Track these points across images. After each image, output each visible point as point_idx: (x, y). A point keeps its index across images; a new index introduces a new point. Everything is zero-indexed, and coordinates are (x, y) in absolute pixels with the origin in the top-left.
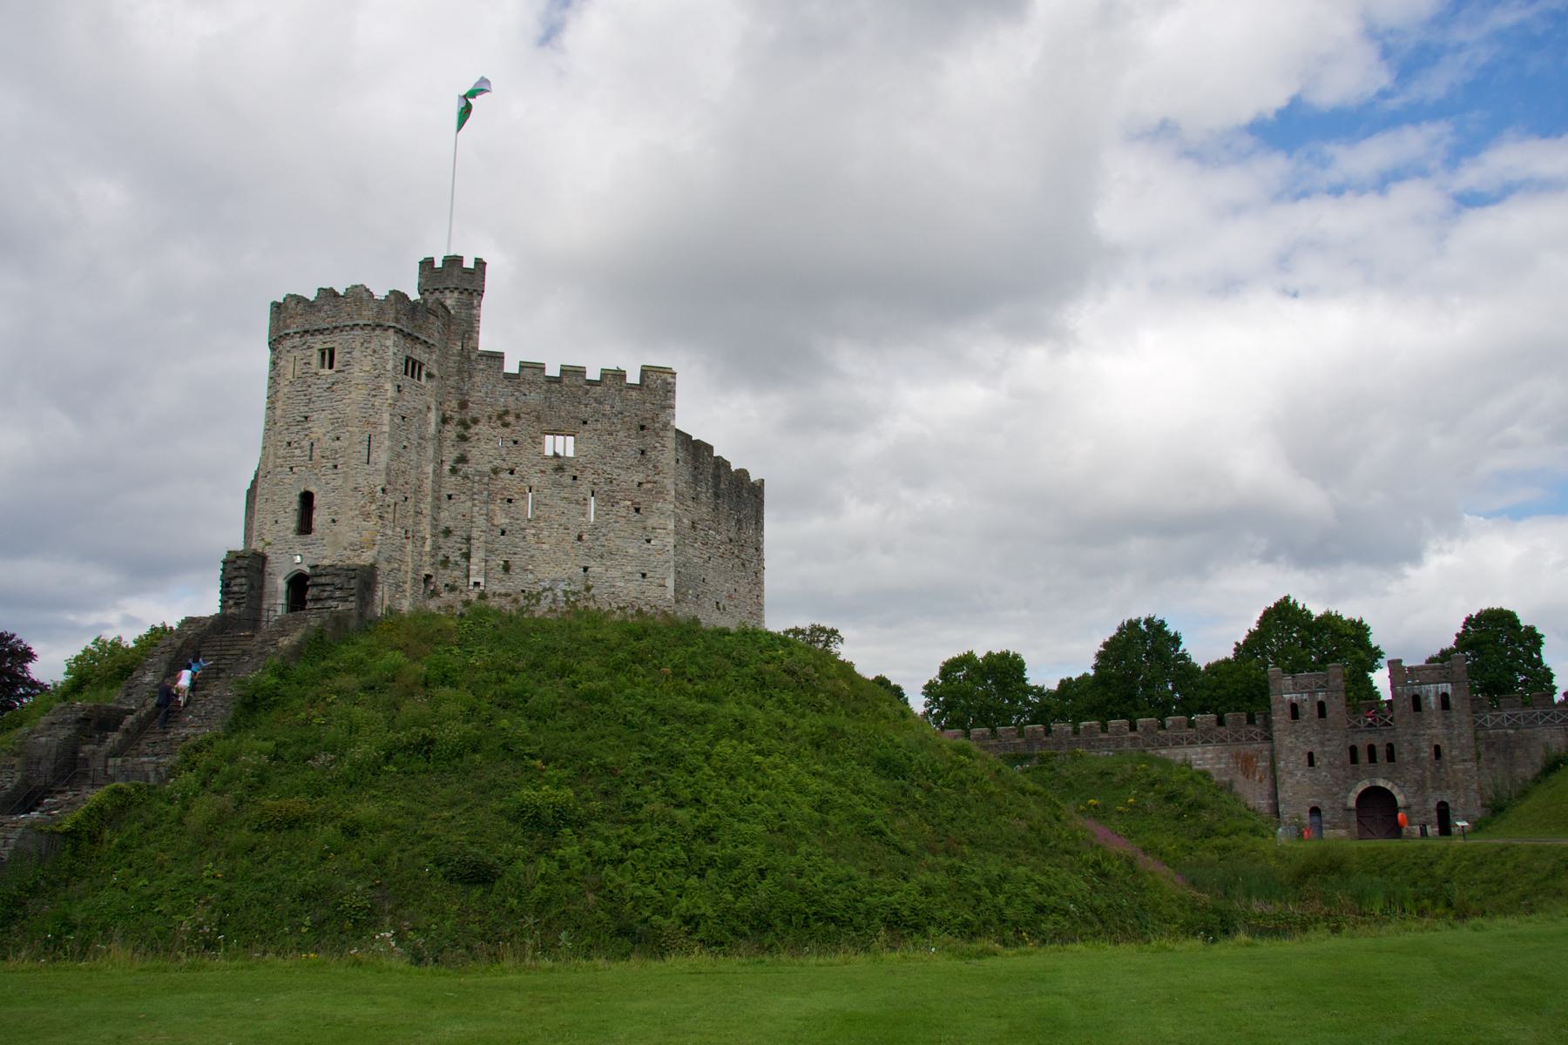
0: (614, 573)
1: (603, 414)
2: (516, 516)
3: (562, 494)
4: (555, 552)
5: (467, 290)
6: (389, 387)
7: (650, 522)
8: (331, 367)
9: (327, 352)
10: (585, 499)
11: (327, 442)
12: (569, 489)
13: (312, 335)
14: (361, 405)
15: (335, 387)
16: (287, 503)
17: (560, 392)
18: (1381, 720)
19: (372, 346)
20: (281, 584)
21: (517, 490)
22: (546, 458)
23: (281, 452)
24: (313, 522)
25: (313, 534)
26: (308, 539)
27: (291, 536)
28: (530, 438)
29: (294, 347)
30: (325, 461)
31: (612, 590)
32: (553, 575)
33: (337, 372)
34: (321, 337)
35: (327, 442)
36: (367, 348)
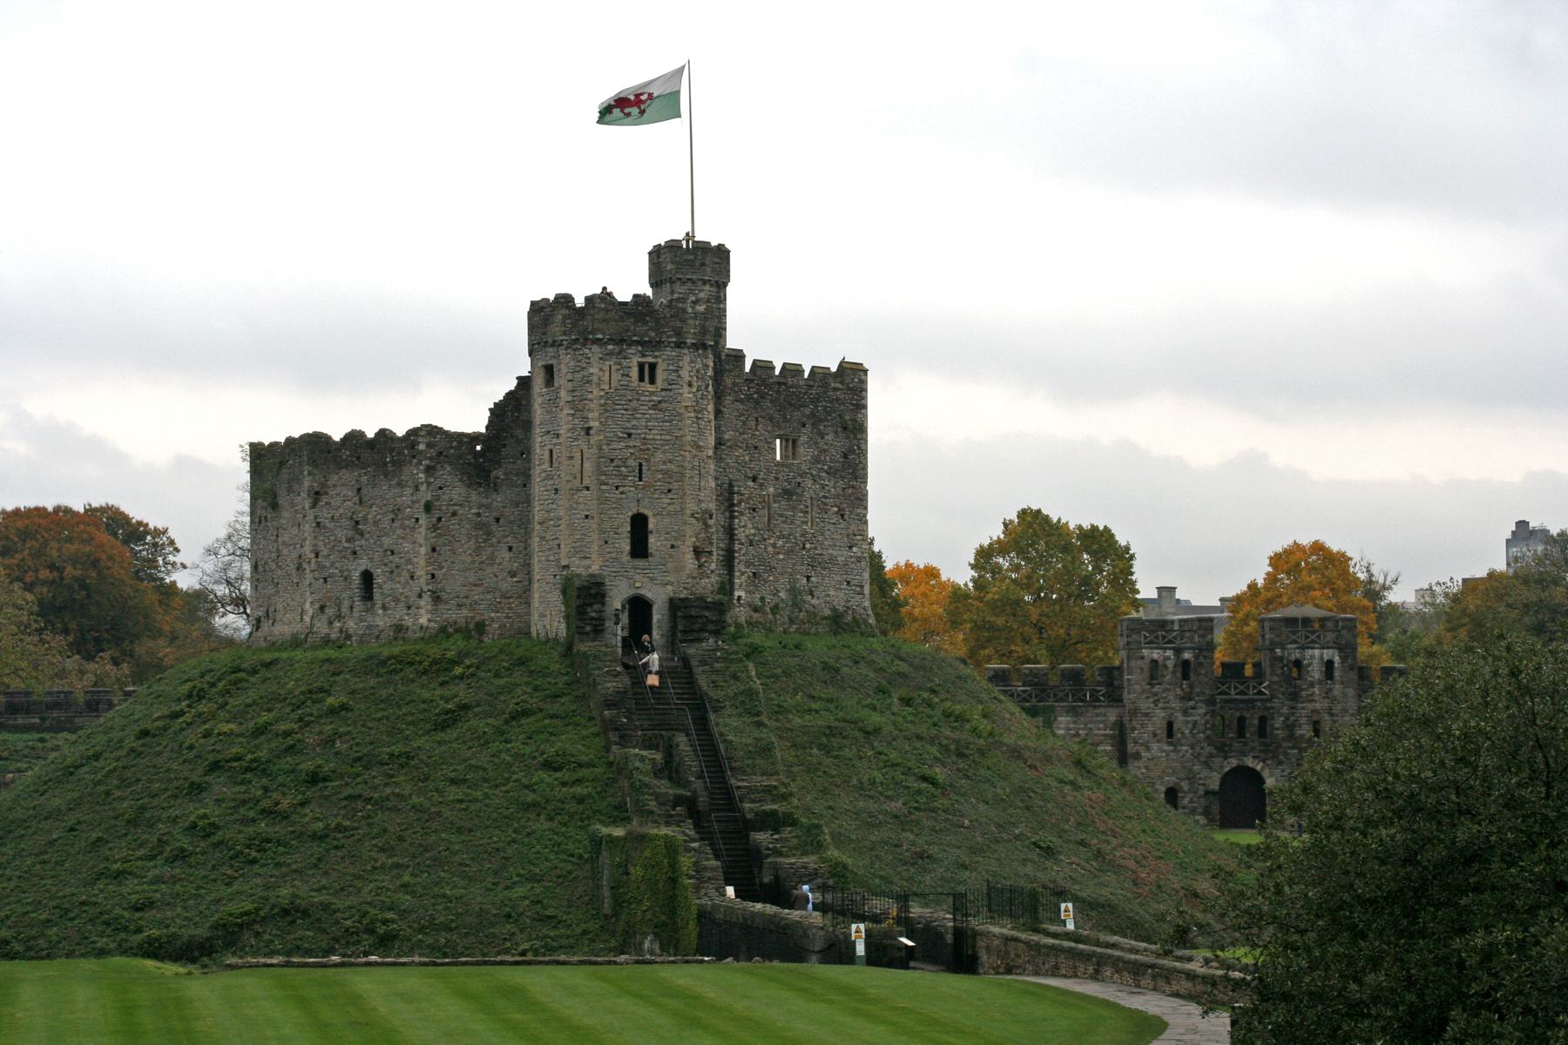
5: (717, 282)
8: (652, 381)
9: (647, 367)
15: (660, 406)
18: (1254, 687)
24: (650, 545)
25: (650, 559)
33: (662, 390)
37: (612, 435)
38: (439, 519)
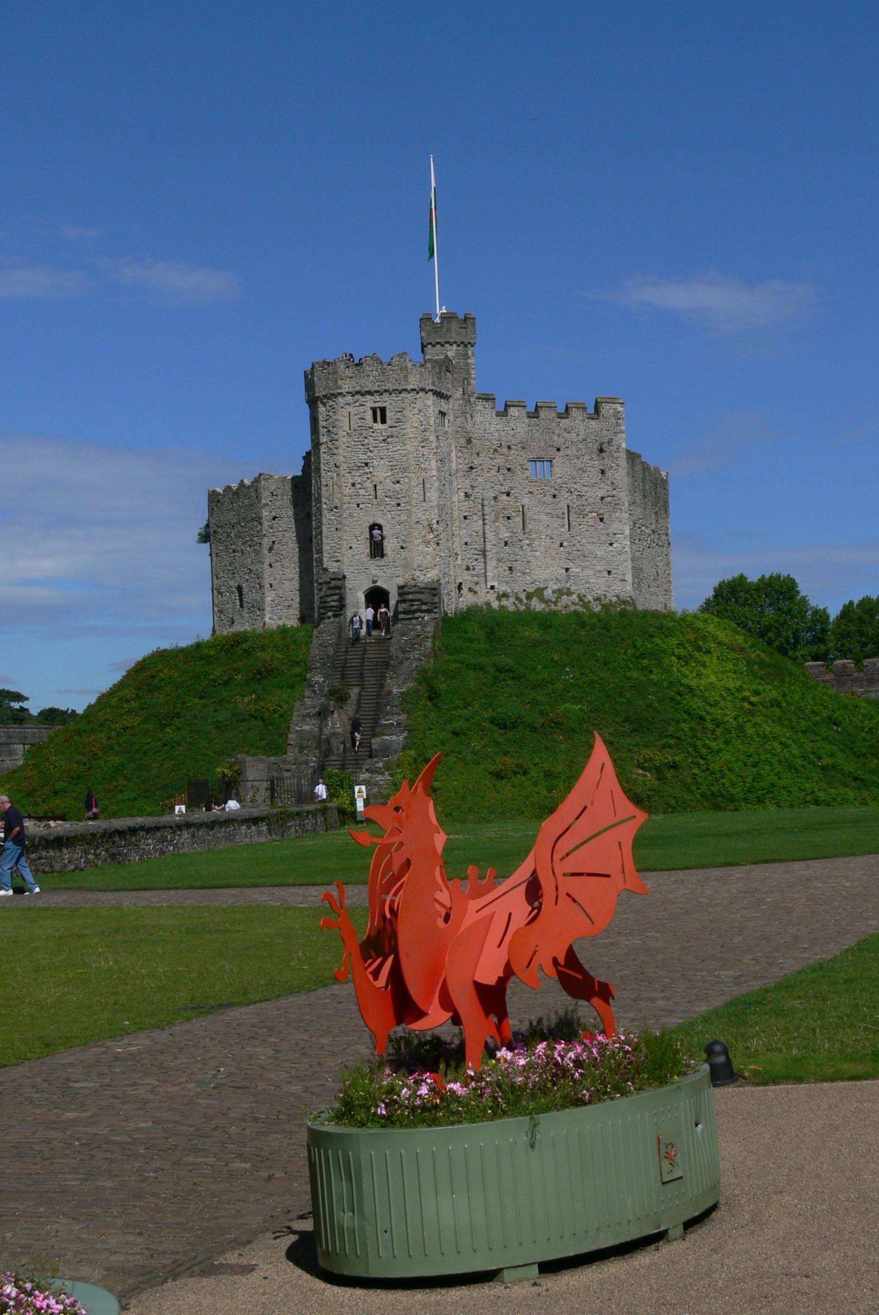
0: (588, 572)
1: (572, 442)
2: (515, 530)
3: (546, 511)
5: (462, 343)
6: (433, 438)
7: (611, 530)
8: (384, 421)
9: (378, 410)
10: (563, 514)
13: (363, 395)
15: (389, 440)
16: (358, 533)
17: (538, 425)
19: (417, 405)
20: (362, 598)
21: (513, 510)
23: (348, 491)
25: (385, 558)
26: (381, 562)
27: (366, 559)
28: (520, 465)
29: (348, 404)
30: (387, 499)
31: (588, 585)
32: (543, 577)
34: (373, 398)
36: (414, 408)
38: (274, 542)
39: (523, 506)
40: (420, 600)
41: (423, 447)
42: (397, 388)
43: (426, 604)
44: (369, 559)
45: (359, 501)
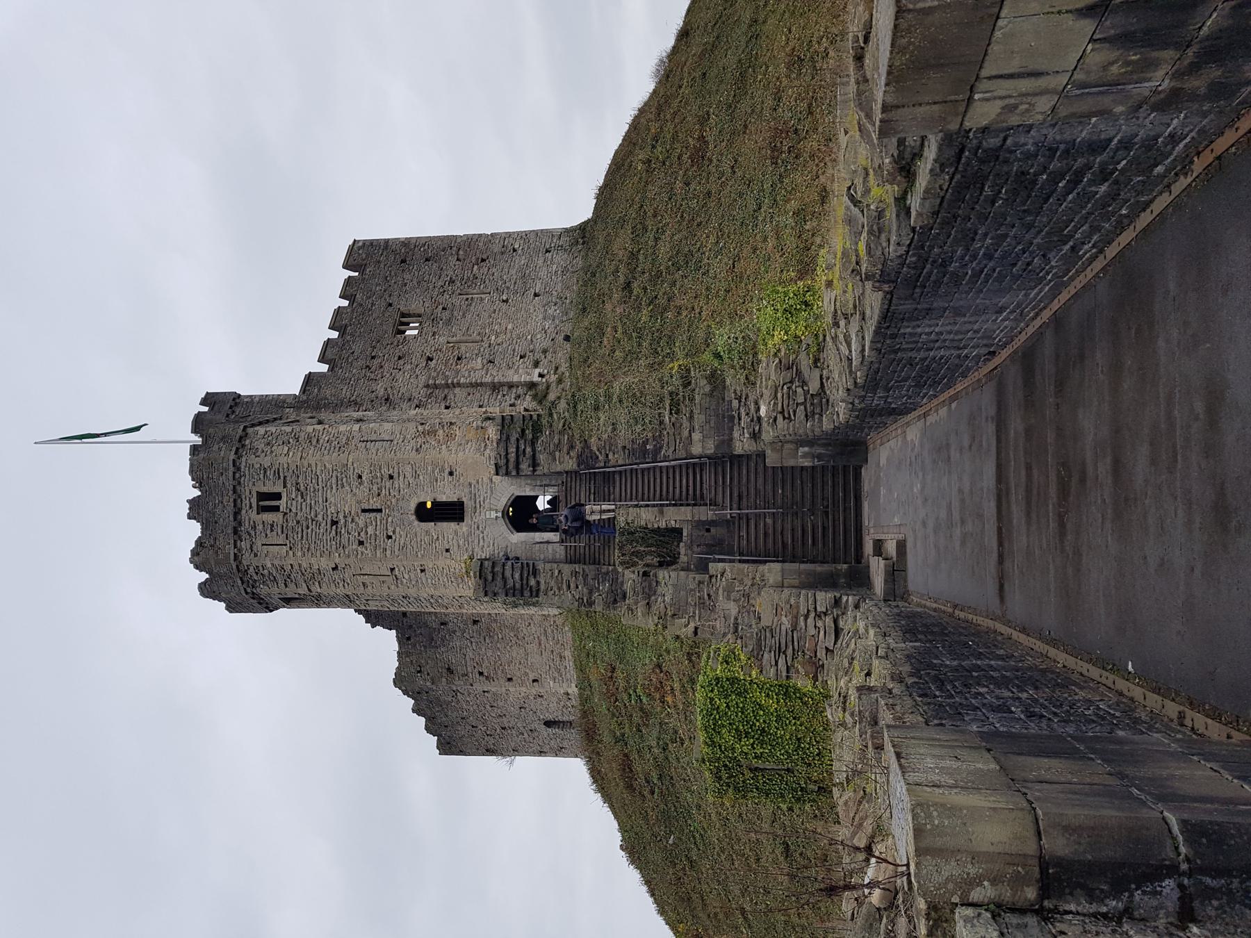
0: (543, 273)
1: (385, 291)
4: (517, 319)
5: (231, 407)
6: (310, 429)
8: (278, 496)
9: (261, 503)
10: (467, 299)
11: (362, 492)
12: (455, 313)
13: (240, 524)
14: (326, 452)
15: (302, 488)
21: (450, 353)
22: (420, 333)
25: (464, 499)
26: (468, 505)
27: (465, 529)
29: (251, 546)
32: (541, 316)
34: (243, 512)
35: (362, 492)
37: (334, 543)
39: (448, 342)
40: (518, 440)
41: (318, 440)
42: (231, 474)
43: (523, 431)
44: (464, 524)
45: (382, 537)
